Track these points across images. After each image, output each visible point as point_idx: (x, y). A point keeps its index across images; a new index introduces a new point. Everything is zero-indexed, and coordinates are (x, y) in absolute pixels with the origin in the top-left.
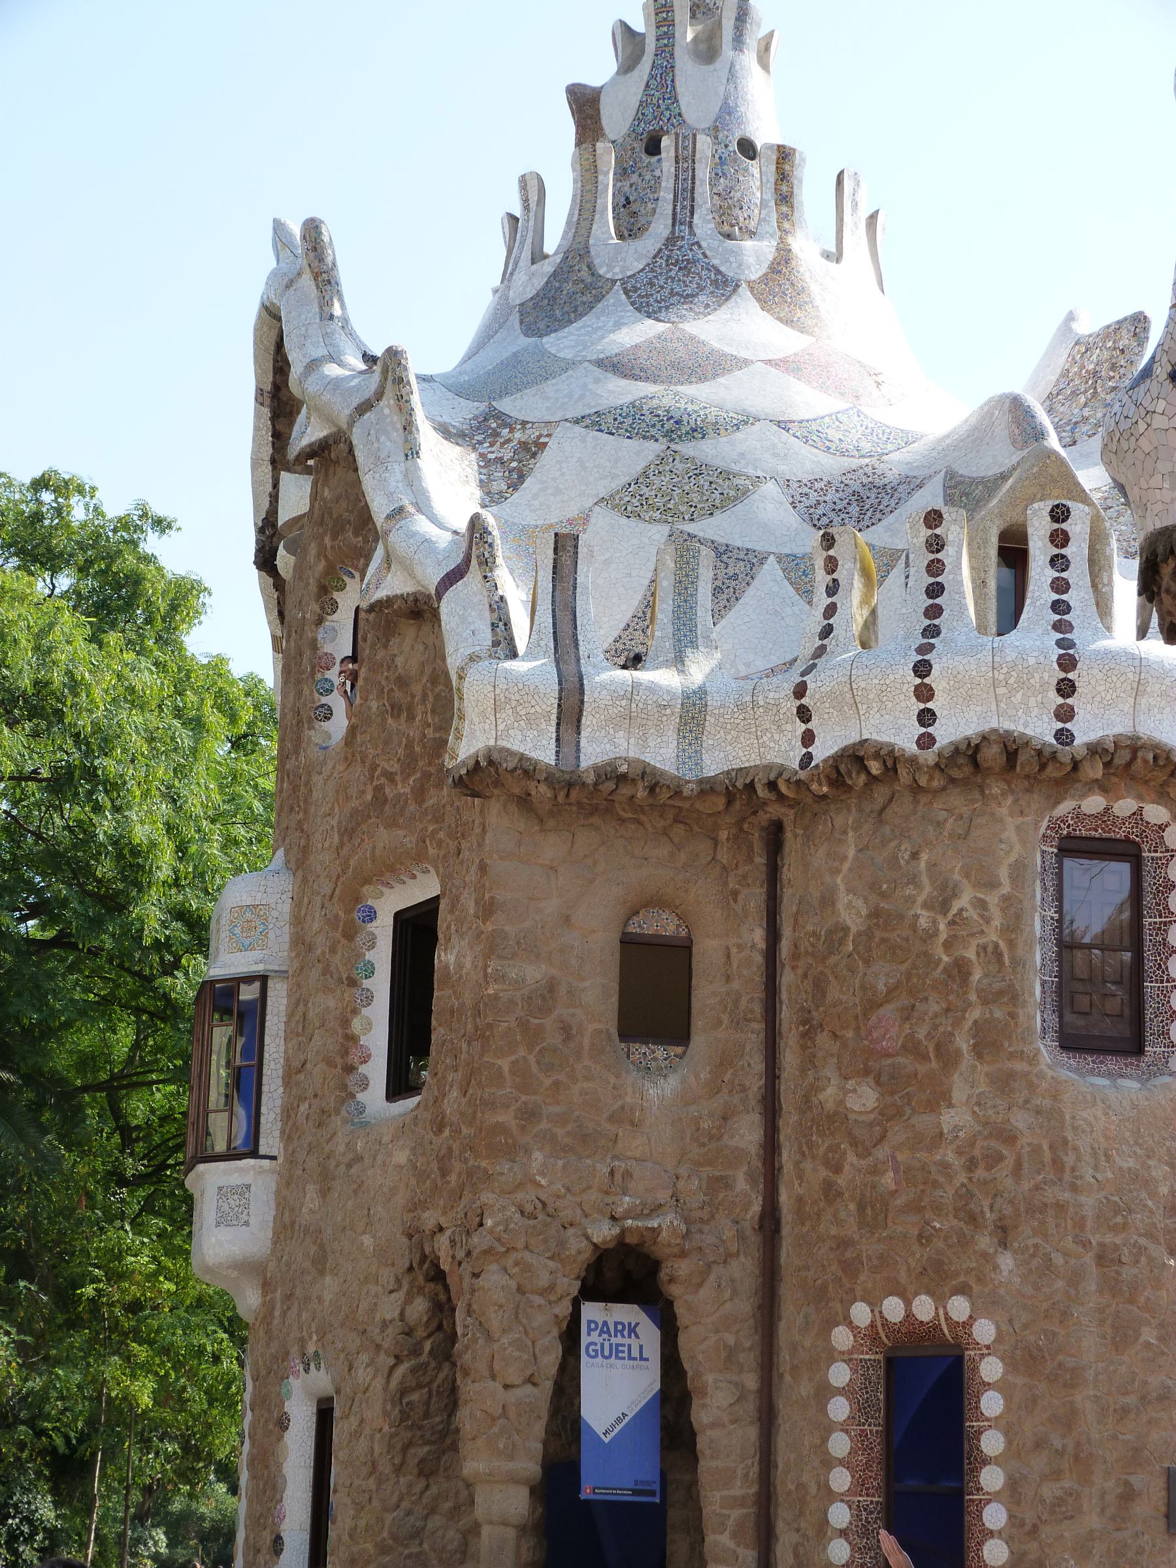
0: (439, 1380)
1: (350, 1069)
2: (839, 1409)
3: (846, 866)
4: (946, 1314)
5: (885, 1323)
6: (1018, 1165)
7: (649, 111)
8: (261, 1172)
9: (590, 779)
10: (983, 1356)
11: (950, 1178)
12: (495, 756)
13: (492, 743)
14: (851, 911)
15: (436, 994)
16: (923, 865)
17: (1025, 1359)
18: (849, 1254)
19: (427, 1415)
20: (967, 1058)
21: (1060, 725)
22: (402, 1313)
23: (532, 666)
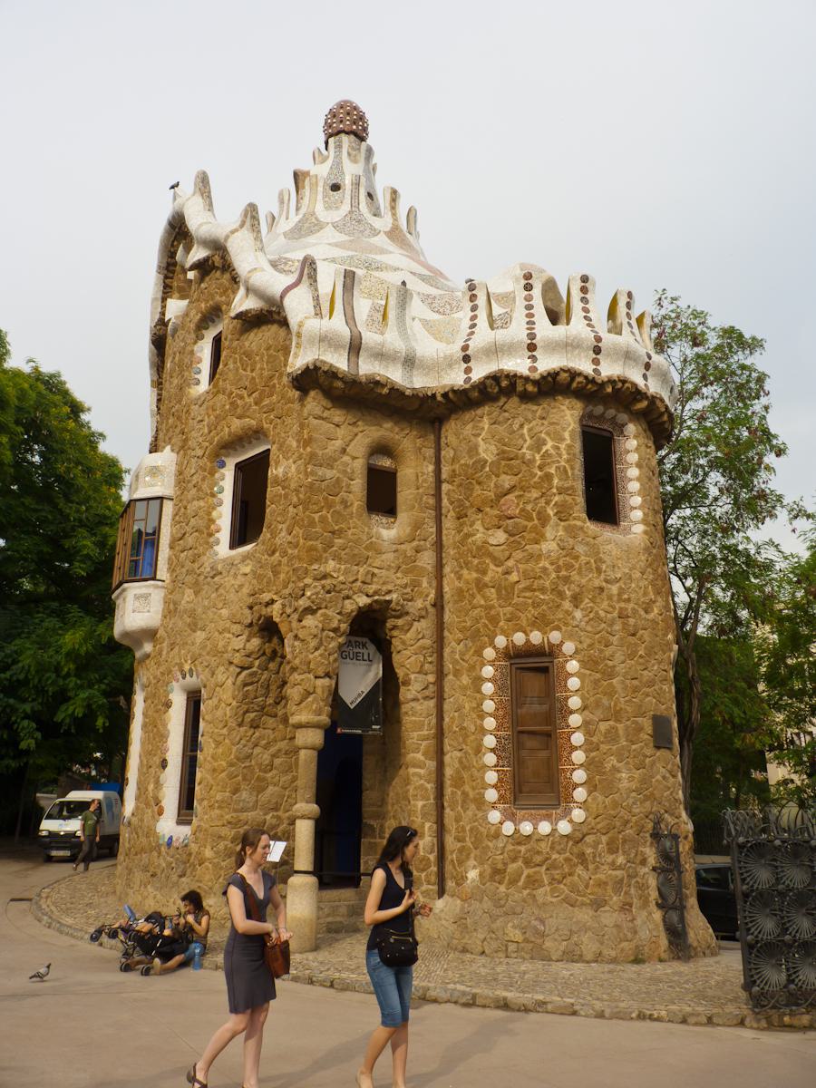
0: (262, 681)
1: (211, 535)
2: (488, 688)
3: (483, 434)
4: (548, 640)
5: (514, 646)
6: (580, 568)
7: (332, 177)
8: (157, 587)
9: (364, 380)
10: (568, 661)
11: (548, 575)
12: (318, 364)
13: (317, 357)
14: (487, 451)
15: (269, 489)
16: (525, 431)
17: (589, 663)
18: (493, 612)
19: (256, 698)
20: (554, 519)
21: (595, 367)
22: (245, 645)
23: (337, 325)
